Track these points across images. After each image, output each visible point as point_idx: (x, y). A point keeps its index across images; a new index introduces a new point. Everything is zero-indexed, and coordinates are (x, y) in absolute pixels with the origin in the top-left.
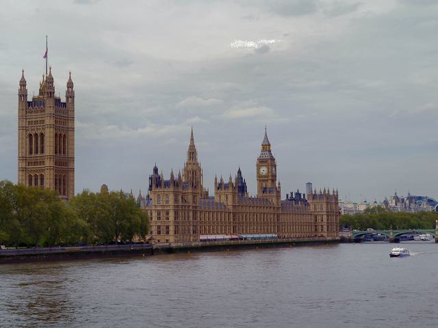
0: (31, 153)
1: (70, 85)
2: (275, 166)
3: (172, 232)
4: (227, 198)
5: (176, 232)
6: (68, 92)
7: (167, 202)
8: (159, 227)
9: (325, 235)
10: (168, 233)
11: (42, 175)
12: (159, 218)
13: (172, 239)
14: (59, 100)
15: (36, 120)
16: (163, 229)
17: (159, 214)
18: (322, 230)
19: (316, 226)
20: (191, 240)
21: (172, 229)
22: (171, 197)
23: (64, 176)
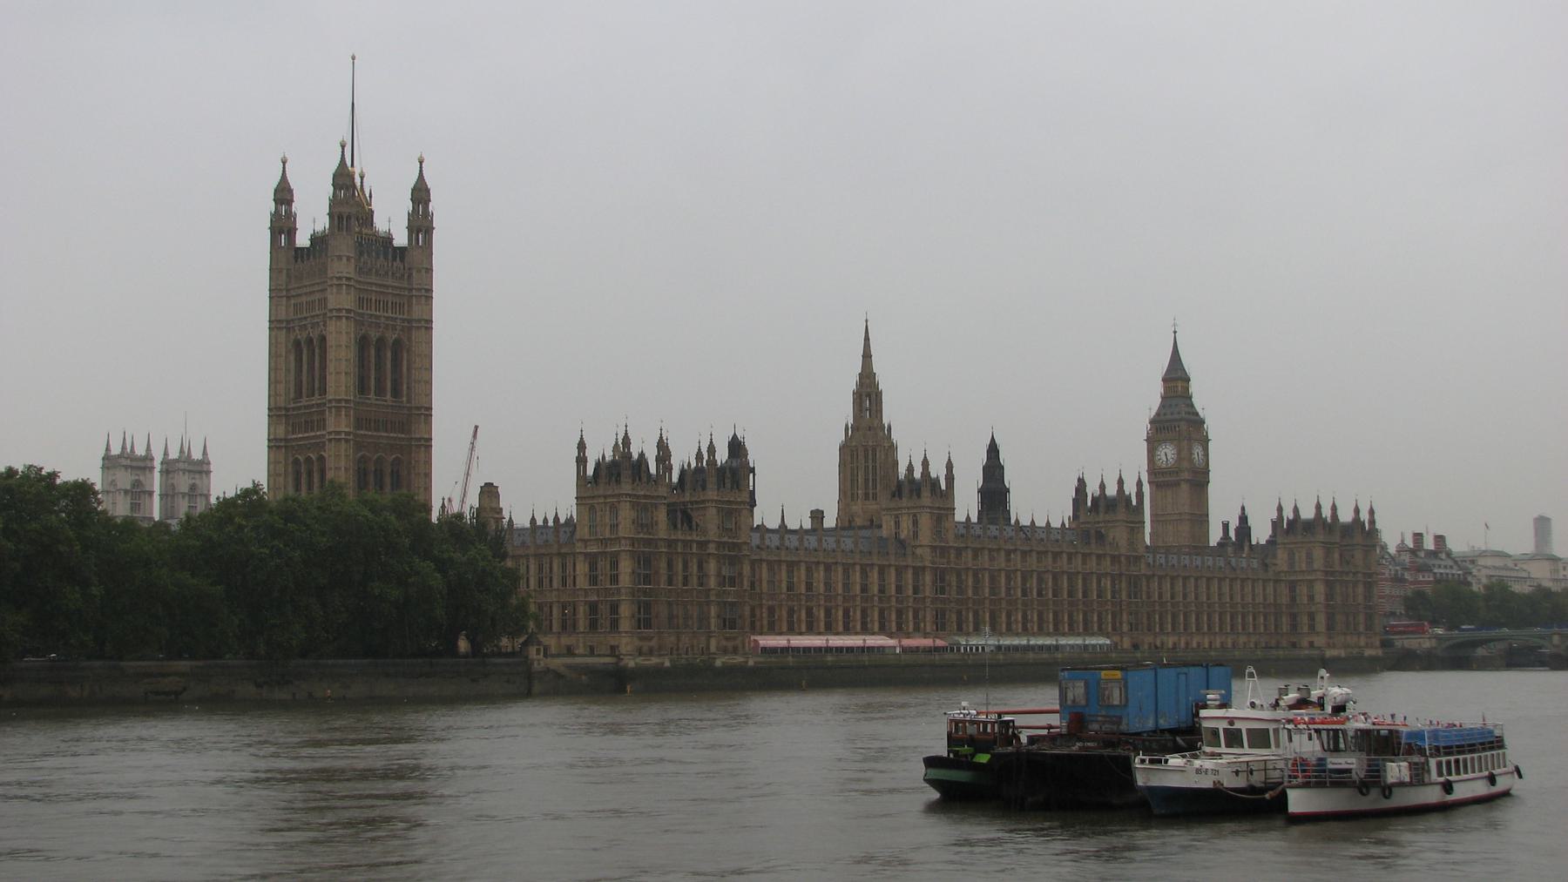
0: (299, 394)
1: (420, 194)
2: (1205, 442)
3: (625, 625)
4: (915, 523)
5: (644, 620)
6: (412, 217)
7: (614, 527)
8: (593, 608)
9: (1320, 641)
10: (615, 624)
11: (322, 459)
12: (593, 580)
13: (626, 644)
14: (388, 239)
15: (310, 299)
16: (604, 610)
17: (593, 566)
18: (1312, 627)
19: (1293, 617)
20: (713, 648)
21: (625, 610)
22: (626, 513)
23: (398, 461)
